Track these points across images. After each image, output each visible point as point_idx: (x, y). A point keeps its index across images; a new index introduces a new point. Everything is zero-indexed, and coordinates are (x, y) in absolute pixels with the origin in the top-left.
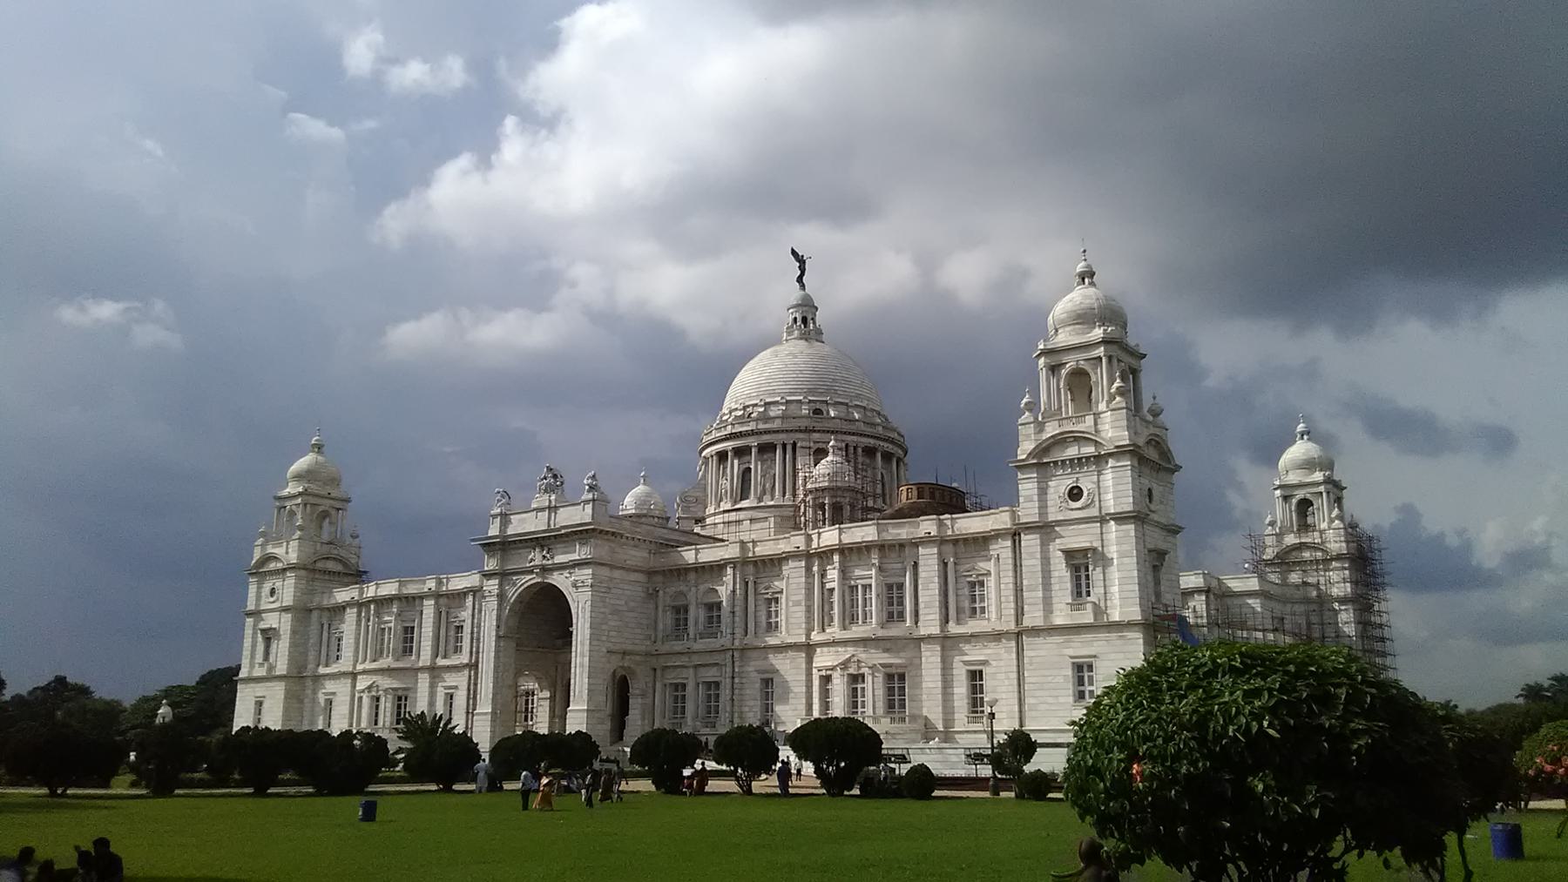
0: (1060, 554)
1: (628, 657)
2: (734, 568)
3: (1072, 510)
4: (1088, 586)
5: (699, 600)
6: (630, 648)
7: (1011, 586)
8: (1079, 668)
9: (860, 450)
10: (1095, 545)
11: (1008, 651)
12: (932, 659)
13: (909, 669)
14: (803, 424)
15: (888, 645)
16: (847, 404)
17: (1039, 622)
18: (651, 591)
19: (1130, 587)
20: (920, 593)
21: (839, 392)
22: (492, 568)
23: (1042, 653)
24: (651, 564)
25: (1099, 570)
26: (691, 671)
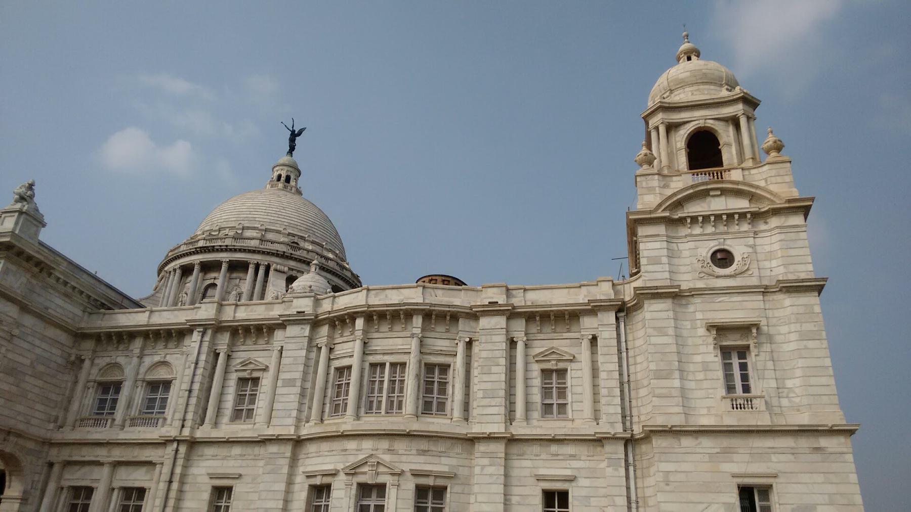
0: (702, 331)
2: (204, 334)
3: (718, 277)
4: (745, 378)
5: (140, 377)
6: (22, 427)
11: (612, 463)
12: (491, 470)
14: (282, 248)
15: (424, 445)
17: (677, 421)
19: (824, 381)
20: (475, 380)
21: (316, 234)
23: (685, 467)
24: (83, 325)
25: (763, 356)
26: (106, 470)
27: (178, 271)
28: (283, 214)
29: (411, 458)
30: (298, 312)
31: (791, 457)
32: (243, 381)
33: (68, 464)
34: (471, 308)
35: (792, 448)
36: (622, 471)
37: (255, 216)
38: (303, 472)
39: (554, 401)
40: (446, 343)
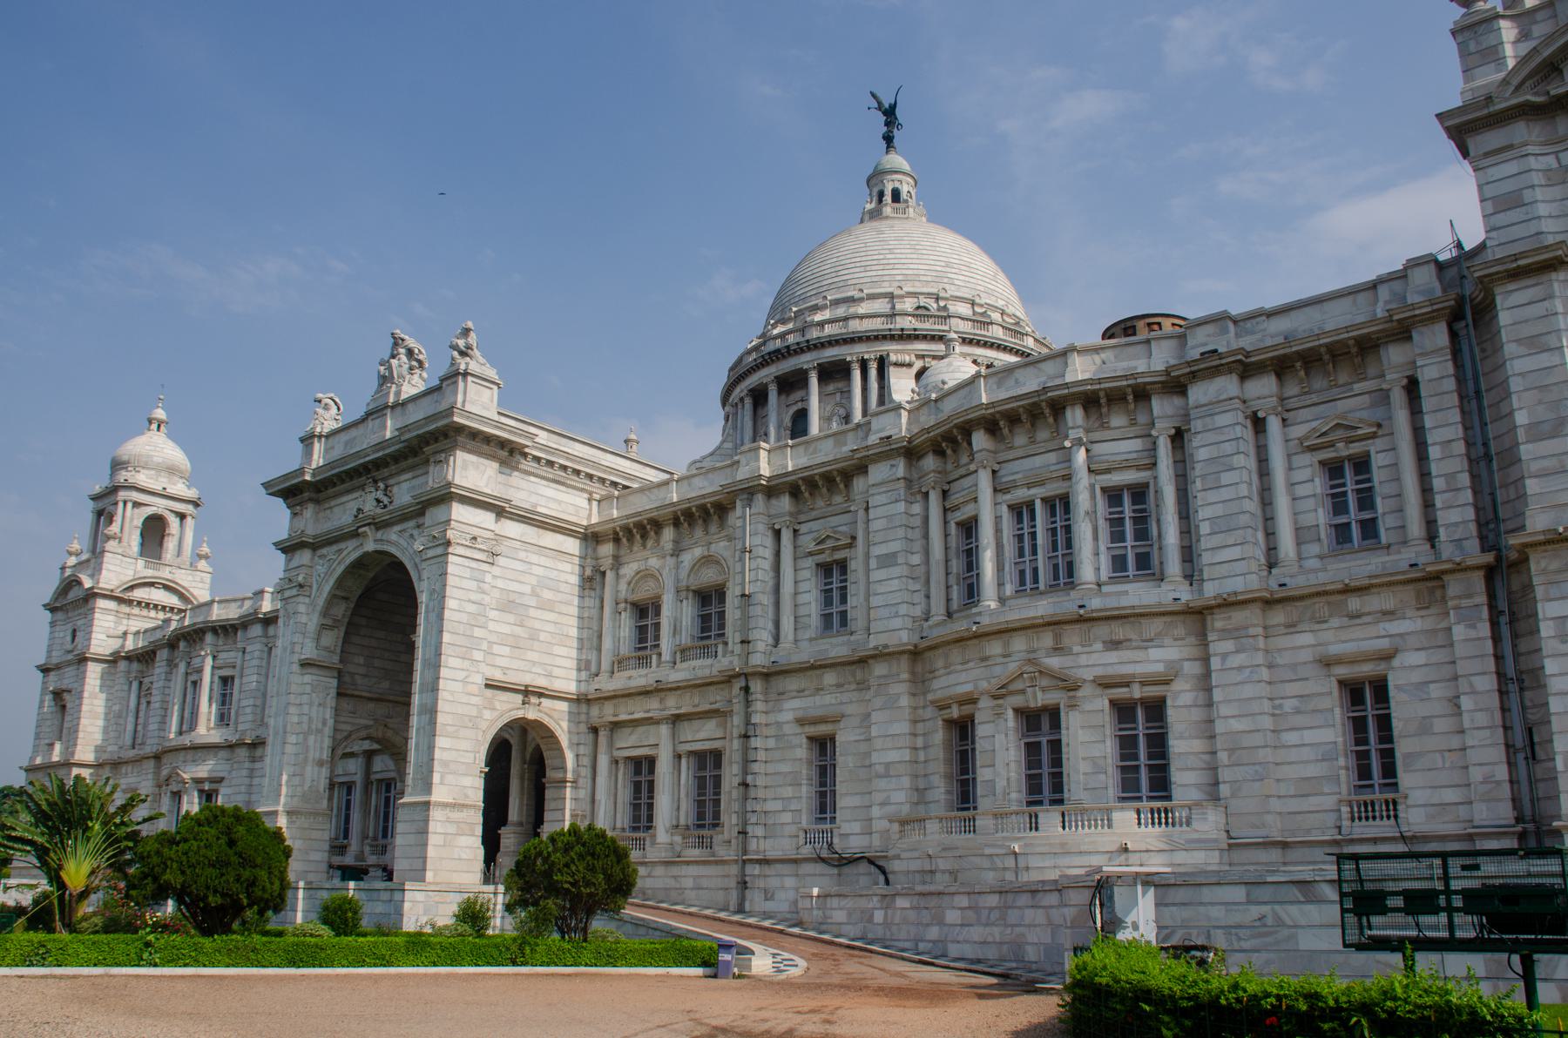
1: (534, 700)
6: (541, 682)
7: (1460, 447)
15: (1119, 631)
26: (664, 730)
29: (1095, 658)
33: (616, 726)
36: (1485, 629)
38: (932, 702)
40: (1136, 444)
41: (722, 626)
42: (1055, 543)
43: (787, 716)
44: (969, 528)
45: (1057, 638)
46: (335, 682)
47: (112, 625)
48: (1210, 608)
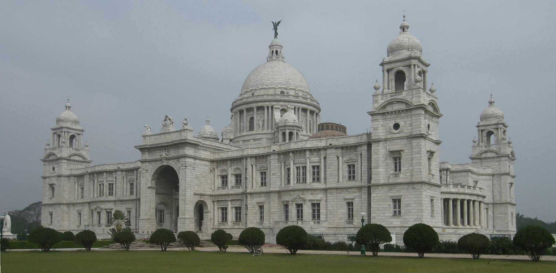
4: (400, 167)
6: (203, 193)
7: (366, 167)
8: (394, 201)
9: (300, 110)
10: (403, 149)
12: (331, 198)
13: (322, 201)
15: (313, 192)
16: (295, 90)
18: (211, 169)
20: (327, 170)
21: (291, 84)
22: (144, 158)
23: (379, 195)
26: (229, 203)
27: (238, 113)
28: (275, 78)
30: (273, 151)
31: (406, 191)
32: (262, 173)
33: (218, 201)
34: (323, 147)
35: (407, 188)
36: (367, 196)
37: (263, 82)
38: (282, 201)
39: (352, 175)
40: (318, 158)
41: (241, 182)
42: (303, 175)
43: (254, 201)
44: (289, 169)
45: (303, 192)
46: (154, 191)
47: (66, 167)
48: (328, 189)
